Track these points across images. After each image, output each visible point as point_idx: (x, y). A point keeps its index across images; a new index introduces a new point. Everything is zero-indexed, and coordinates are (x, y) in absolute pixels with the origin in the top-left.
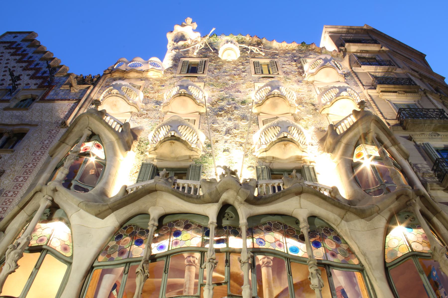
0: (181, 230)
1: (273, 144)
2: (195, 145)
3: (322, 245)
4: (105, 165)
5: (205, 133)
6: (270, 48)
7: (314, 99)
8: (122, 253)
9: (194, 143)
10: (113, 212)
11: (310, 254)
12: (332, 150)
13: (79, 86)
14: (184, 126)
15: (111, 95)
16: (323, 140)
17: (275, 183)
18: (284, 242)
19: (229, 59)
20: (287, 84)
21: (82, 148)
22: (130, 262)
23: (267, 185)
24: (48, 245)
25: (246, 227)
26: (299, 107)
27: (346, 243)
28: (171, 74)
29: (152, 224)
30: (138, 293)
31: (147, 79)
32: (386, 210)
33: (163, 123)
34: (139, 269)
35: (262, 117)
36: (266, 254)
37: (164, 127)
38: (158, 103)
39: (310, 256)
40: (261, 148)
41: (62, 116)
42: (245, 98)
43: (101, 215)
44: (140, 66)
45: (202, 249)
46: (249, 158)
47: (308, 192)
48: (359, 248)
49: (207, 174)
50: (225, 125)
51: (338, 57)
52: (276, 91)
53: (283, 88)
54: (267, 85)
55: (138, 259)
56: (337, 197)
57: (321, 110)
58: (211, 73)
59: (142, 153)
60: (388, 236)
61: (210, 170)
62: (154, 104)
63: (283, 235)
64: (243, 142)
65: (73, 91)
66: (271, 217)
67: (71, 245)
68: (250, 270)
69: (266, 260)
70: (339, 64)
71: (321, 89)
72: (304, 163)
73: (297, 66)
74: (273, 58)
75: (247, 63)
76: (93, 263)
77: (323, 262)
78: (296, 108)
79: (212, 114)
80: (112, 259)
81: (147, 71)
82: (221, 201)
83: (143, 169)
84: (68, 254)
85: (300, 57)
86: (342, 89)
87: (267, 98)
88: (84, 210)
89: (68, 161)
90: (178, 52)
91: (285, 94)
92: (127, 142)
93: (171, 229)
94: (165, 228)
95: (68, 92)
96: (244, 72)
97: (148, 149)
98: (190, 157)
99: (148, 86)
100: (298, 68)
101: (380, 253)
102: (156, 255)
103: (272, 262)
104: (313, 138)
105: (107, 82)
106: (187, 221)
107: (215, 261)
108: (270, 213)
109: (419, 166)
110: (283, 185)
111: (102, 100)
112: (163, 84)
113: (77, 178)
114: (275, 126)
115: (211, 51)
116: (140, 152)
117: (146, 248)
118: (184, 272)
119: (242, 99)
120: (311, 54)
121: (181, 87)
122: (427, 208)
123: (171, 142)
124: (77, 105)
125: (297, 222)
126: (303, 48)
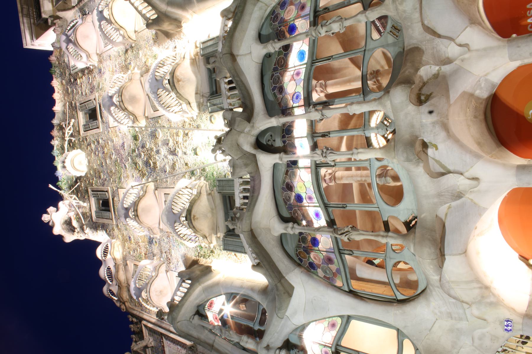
0: (294, 194)
1: (179, 96)
2: (194, 190)
3: (291, 23)
4: (232, 293)
5: (178, 180)
6: (64, 113)
7: (120, 50)
8: (330, 261)
9: (191, 191)
10: (284, 277)
11: (304, 36)
12: (177, 22)
13: (145, 337)
14: (173, 207)
15: (149, 299)
16: (168, 35)
17: (225, 88)
18: (294, 69)
19: (86, 162)
20: (105, 86)
21: (216, 324)
22: (339, 249)
23: (228, 98)
24: (331, 346)
25: (280, 117)
26: (132, 68)
28: (114, 230)
29: (292, 230)
30: (372, 235)
31: (125, 259)
33: (172, 232)
34: (345, 239)
35: (150, 113)
36: (310, 90)
37: (177, 231)
38: (151, 241)
39: (307, 36)
40: (186, 110)
41: (184, 351)
42: (130, 137)
43: (289, 291)
44: (110, 269)
45: (314, 167)
46: (200, 123)
47: (231, 47)
49: (226, 172)
50: (166, 157)
51: (62, 26)
52: (115, 100)
53: (110, 91)
54: (110, 112)
55: (334, 241)
56: (233, 10)
57: (131, 41)
58: (106, 182)
59: (212, 252)
61: (222, 168)
62: (153, 245)
63: (286, 71)
64: (182, 133)
66: (266, 88)
67: (327, 319)
68: (331, 107)
69: (318, 89)
70: (70, 23)
71: (106, 44)
72: (198, 55)
73: (82, 77)
74: (76, 108)
75: (87, 140)
76: (345, 291)
77: (312, 19)
78: (133, 72)
79: (155, 175)
80: (338, 271)
81: (114, 259)
83: (231, 248)
84: (339, 321)
85: (70, 74)
86: (101, 17)
87: (125, 109)
88: (286, 311)
89: (232, 338)
90: (87, 225)
91: (118, 88)
92: (202, 271)
93: (295, 206)
94: (294, 214)
96: (98, 142)
97: (207, 246)
98: (209, 194)
99: (132, 256)
100: (84, 75)
102: (327, 221)
103: (320, 82)
104: (166, 47)
105: (136, 306)
106: (283, 188)
107: (325, 150)
108: (261, 90)
110: (226, 78)
111: (157, 308)
112: (128, 238)
113: (251, 325)
114: (158, 97)
115: (78, 186)
116: (211, 254)
117: (320, 233)
118: (345, 185)
119: (132, 141)
120: (64, 60)
121: (127, 216)
123: (194, 220)
124: (168, 336)
125: (268, 56)
126: (58, 72)
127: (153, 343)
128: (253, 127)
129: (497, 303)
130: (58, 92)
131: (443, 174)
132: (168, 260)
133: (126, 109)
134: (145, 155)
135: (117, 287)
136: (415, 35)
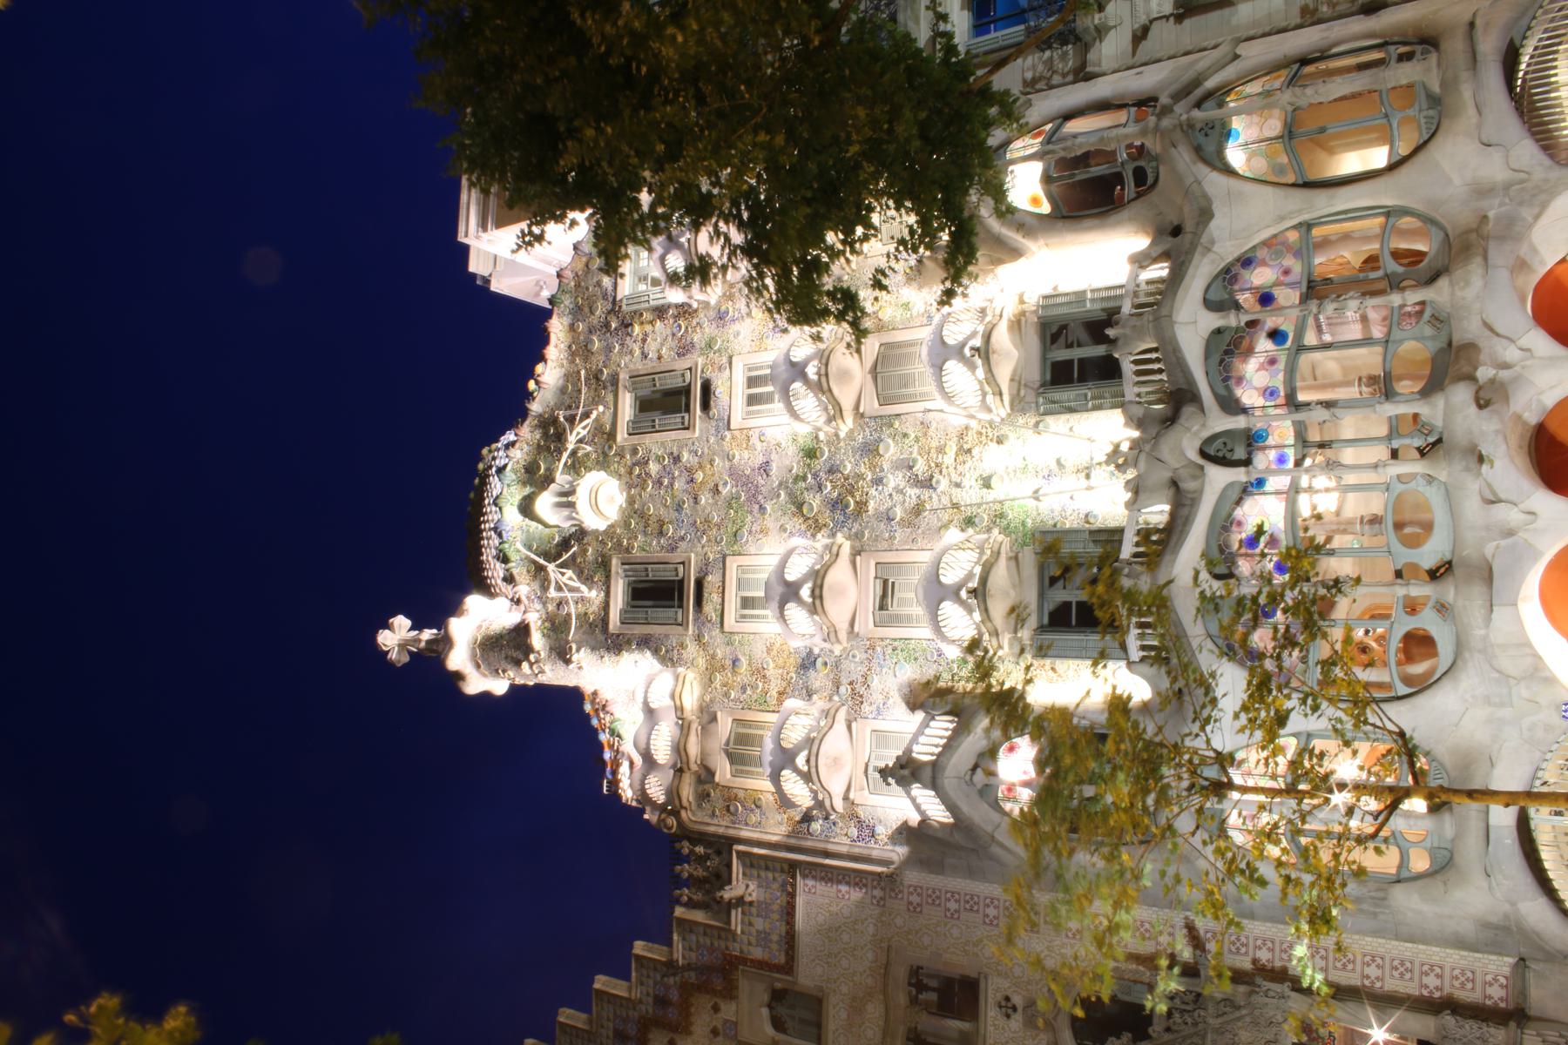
19: (621, 499)
42: (792, 450)
52: (811, 371)
56: (1154, 255)
58: (683, 545)
64: (955, 448)
75: (635, 451)
81: (679, 709)
82: (1201, 461)
95: (754, 910)
96: (677, 459)
101: (1279, 192)
105: (713, 815)
109: (1029, 75)
112: (728, 663)
122: (1188, 94)
128: (1204, 425)
129: (1551, 680)
131: (1493, 502)
132: (857, 699)
133: (830, 390)
134: (834, 488)
136: (1469, 329)
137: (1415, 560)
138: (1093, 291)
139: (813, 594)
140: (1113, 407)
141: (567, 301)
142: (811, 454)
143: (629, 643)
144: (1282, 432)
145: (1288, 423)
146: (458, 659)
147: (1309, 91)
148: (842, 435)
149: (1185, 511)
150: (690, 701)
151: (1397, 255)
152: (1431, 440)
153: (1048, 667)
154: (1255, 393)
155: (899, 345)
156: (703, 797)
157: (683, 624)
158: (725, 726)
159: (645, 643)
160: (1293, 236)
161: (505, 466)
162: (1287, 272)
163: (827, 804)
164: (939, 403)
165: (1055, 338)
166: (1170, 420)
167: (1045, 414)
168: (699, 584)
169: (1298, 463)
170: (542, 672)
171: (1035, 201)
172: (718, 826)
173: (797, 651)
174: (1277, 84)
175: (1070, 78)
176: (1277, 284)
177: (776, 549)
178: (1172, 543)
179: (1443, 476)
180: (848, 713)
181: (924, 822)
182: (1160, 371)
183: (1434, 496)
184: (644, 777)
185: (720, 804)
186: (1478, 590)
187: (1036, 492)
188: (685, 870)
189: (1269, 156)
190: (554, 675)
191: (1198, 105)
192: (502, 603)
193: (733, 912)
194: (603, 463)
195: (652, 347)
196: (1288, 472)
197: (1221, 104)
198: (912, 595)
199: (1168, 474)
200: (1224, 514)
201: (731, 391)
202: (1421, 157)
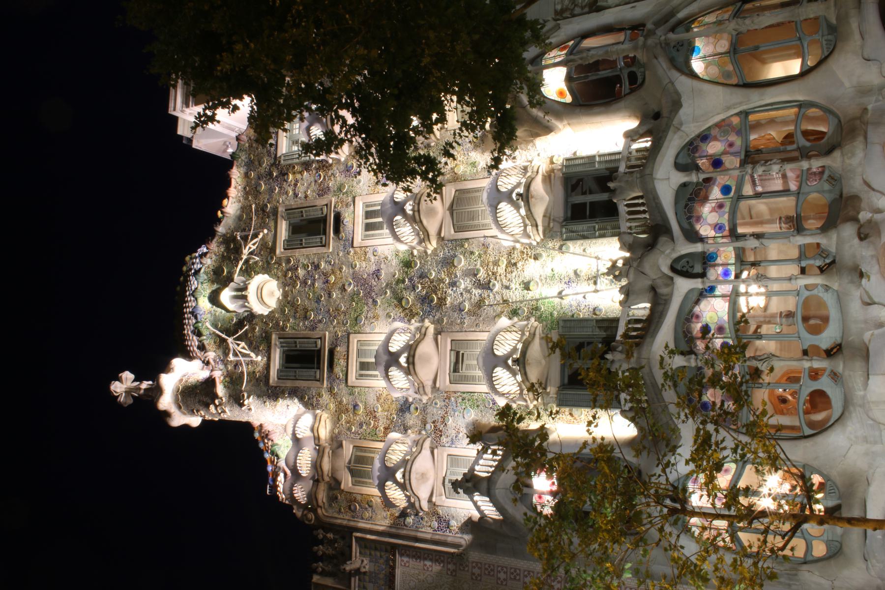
1: (530, 214)
15: (407, 482)
19: (278, 294)
27: (709, 128)
32: (669, 74)
40: (531, 234)
42: (395, 262)
48: (719, 114)
50: (468, 291)
52: (408, 208)
56: (641, 132)
58: (321, 326)
60: (701, 76)
64: (505, 262)
65: (367, 567)
73: (301, 173)
75: (288, 261)
77: (743, 157)
81: (317, 439)
82: (671, 274)
95: (367, 578)
96: (317, 267)
99: (356, 433)
105: (340, 510)
109: (559, 7)
112: (351, 407)
119: (398, 268)
122: (667, 21)
126: (243, 158)
127: (367, 567)
128: (673, 250)
130: (235, 188)
131: (869, 304)
132: (438, 433)
133: (421, 222)
134: (423, 288)
135: (311, 482)
136: (855, 185)
137: (817, 343)
138: (600, 156)
139: (408, 362)
140: (613, 235)
141: (243, 157)
142: (408, 264)
143: (283, 393)
144: (727, 254)
145: (731, 249)
146: (166, 402)
147: (747, 21)
148: (429, 252)
149: (660, 308)
150: (324, 433)
151: (806, 134)
152: (828, 261)
153: (567, 413)
154: (709, 228)
155: (468, 191)
156: (332, 499)
157: (321, 380)
158: (348, 450)
159: (294, 393)
160: (736, 121)
161: (200, 269)
162: (731, 145)
163: (417, 505)
164: (494, 231)
165: (574, 188)
166: (651, 246)
167: (567, 240)
168: (332, 353)
169: (737, 276)
170: (224, 412)
171: (561, 94)
172: (343, 519)
173: (397, 399)
174: (726, 16)
175: (587, 10)
176: (725, 153)
177: (386, 330)
178: (651, 330)
179: (835, 286)
180: (432, 442)
181: (483, 517)
182: (644, 212)
183: (829, 299)
184: (292, 486)
185: (344, 504)
186: (859, 364)
187: (560, 293)
188: (320, 549)
189: (720, 66)
190: (231, 414)
191: (673, 30)
192: (197, 364)
193: (353, 579)
194: (266, 269)
195: (301, 189)
196: (730, 282)
197: (688, 29)
198: (475, 362)
199: (650, 283)
200: (687, 310)
201: (355, 220)
202: (823, 67)
